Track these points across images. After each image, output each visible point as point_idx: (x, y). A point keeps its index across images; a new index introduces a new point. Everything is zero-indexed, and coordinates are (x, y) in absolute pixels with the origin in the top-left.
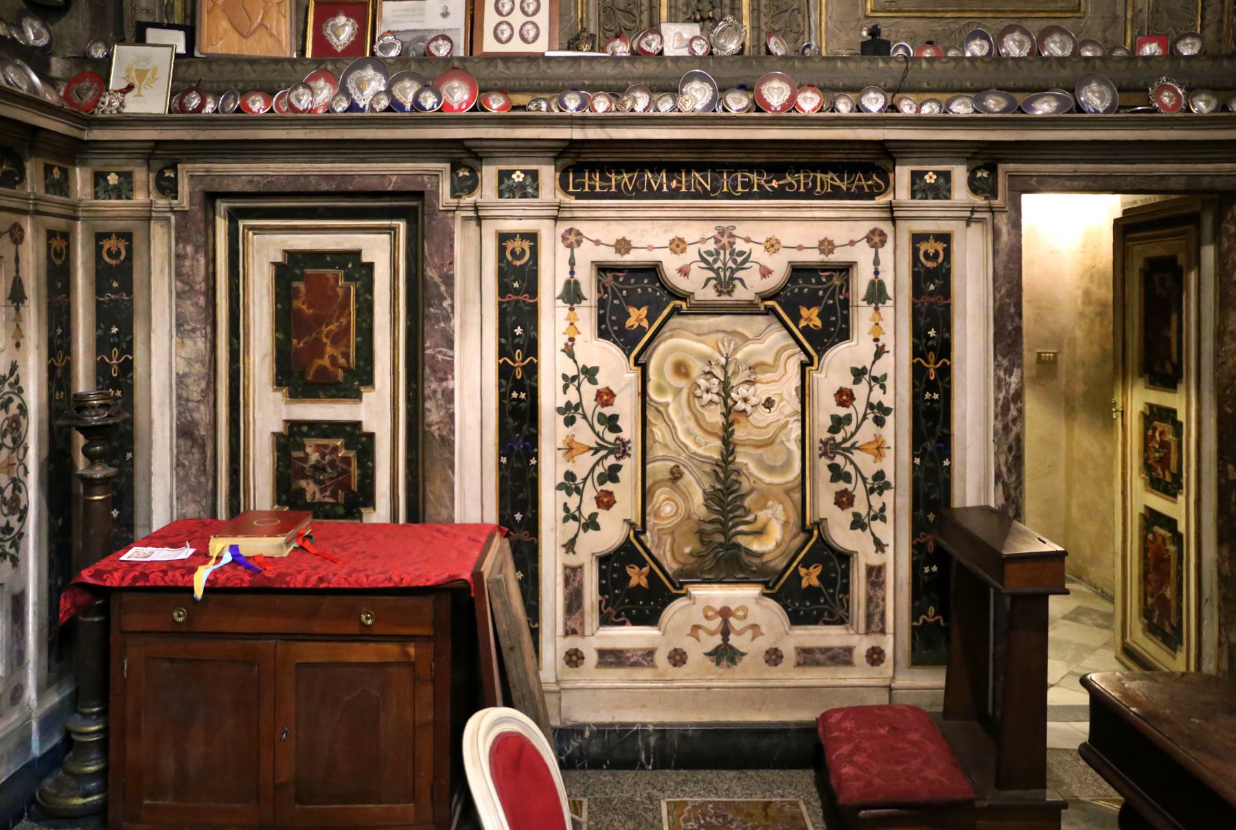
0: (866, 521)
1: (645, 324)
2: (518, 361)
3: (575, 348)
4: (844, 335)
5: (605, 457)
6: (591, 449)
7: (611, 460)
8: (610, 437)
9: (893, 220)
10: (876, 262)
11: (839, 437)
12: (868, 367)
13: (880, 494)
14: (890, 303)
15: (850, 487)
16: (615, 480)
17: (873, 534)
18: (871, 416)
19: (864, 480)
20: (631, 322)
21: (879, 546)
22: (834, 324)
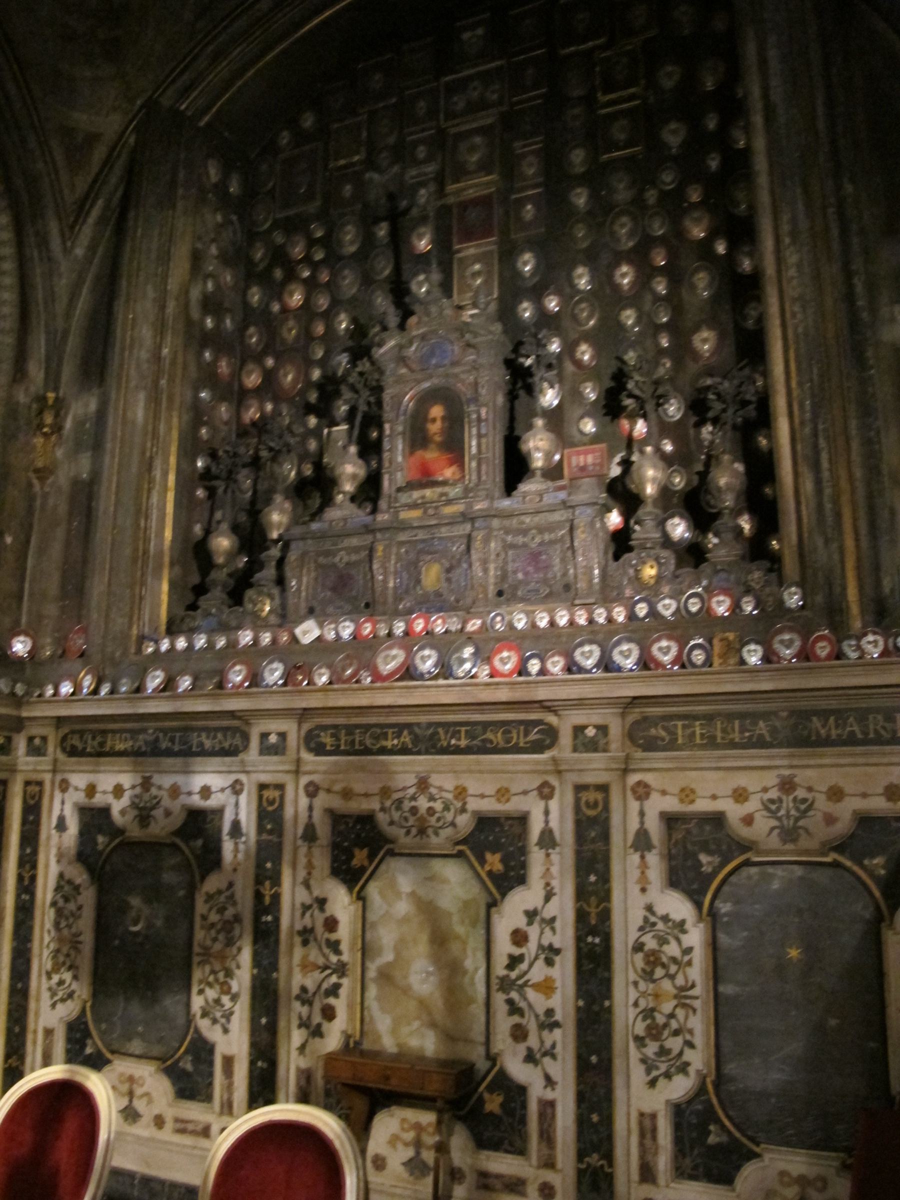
0: (538, 1056)
1: (366, 863)
2: (267, 891)
3: (312, 882)
4: (522, 880)
5: (331, 974)
6: (319, 967)
7: (334, 979)
8: (334, 959)
9: (559, 772)
10: (547, 813)
11: (514, 975)
12: (540, 908)
13: (551, 1030)
14: (558, 849)
15: (524, 1022)
16: (336, 995)
17: (544, 1069)
18: (543, 956)
19: (537, 1016)
20: (356, 862)
21: (549, 1082)
22: (513, 868)
